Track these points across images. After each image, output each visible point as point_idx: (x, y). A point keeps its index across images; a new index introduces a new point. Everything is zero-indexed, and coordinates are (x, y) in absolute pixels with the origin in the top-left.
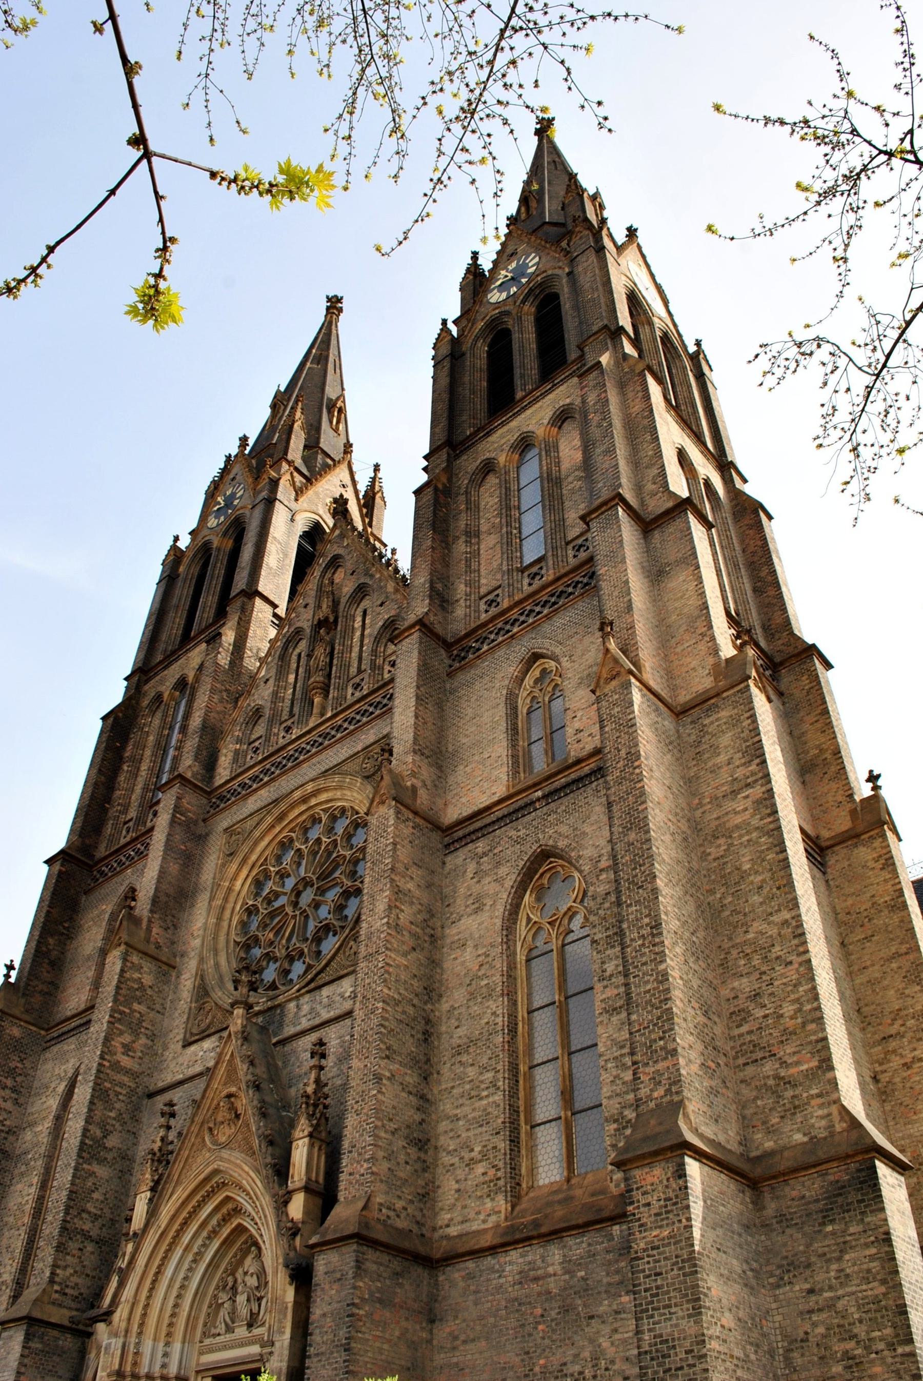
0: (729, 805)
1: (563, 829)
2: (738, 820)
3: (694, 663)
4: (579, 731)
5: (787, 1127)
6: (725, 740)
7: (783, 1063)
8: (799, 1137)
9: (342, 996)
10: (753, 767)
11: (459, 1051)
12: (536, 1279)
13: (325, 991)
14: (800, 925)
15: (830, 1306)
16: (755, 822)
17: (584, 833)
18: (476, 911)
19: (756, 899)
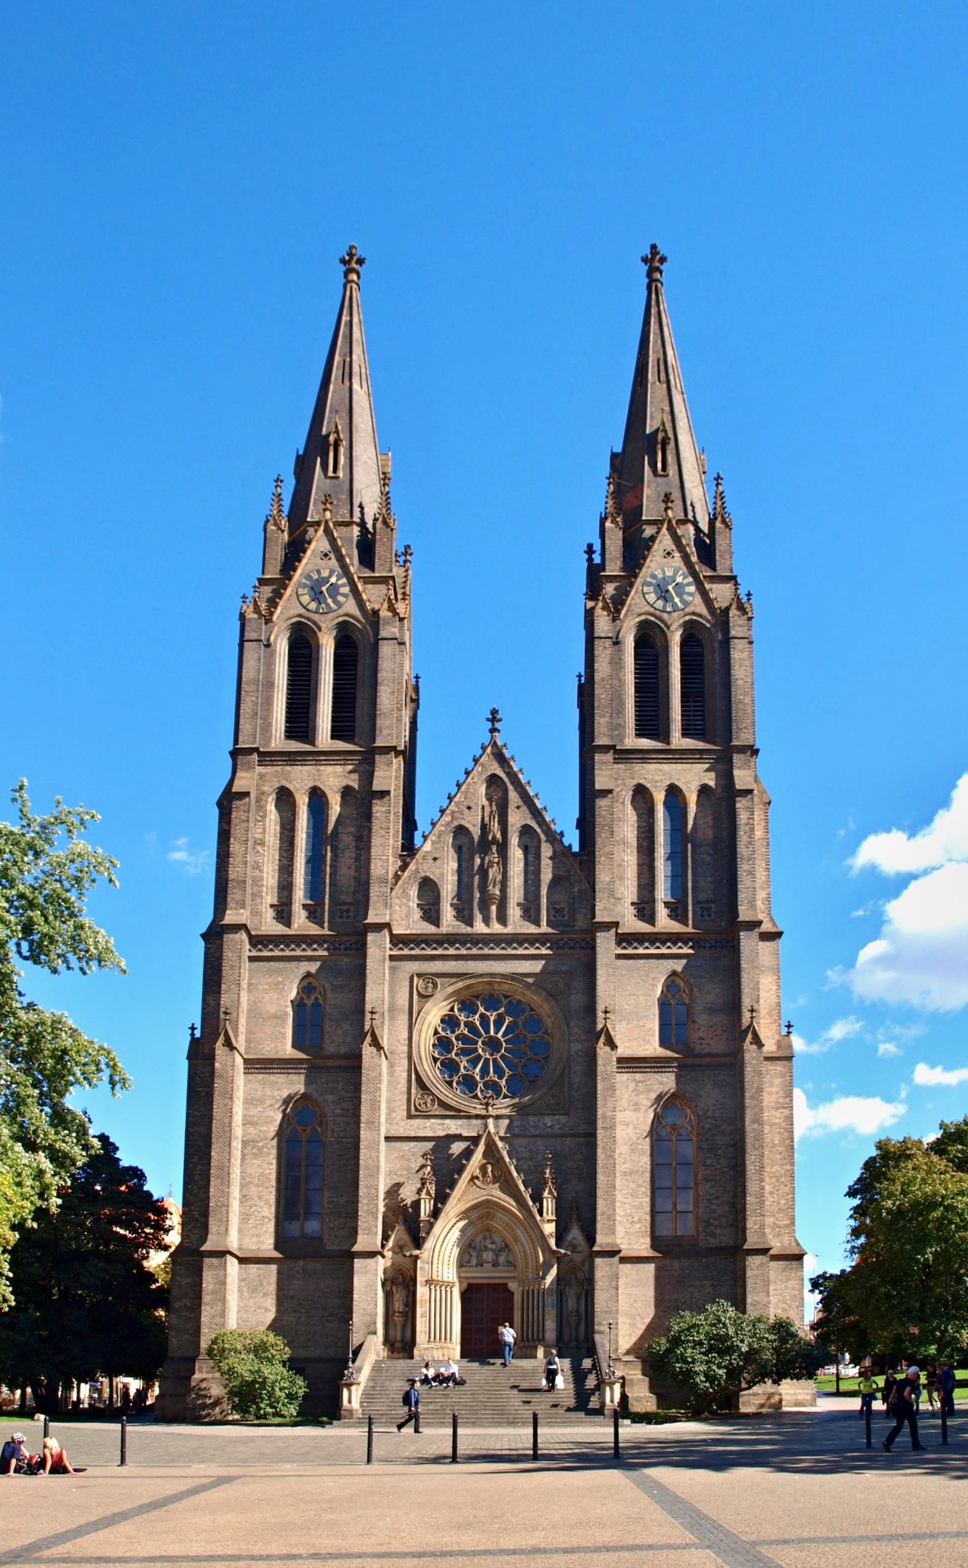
0: (773, 1112)
1: (689, 1088)
2: (777, 1121)
3: (769, 1034)
4: (701, 1038)
5: (775, 1240)
6: (777, 1081)
7: (777, 1219)
8: (778, 1244)
9: (545, 1124)
10: (787, 1100)
11: (625, 1174)
12: (667, 1270)
13: (531, 1118)
14: (793, 1173)
15: (781, 1294)
16: (784, 1125)
17: (701, 1096)
18: (635, 1110)
19: (778, 1156)
